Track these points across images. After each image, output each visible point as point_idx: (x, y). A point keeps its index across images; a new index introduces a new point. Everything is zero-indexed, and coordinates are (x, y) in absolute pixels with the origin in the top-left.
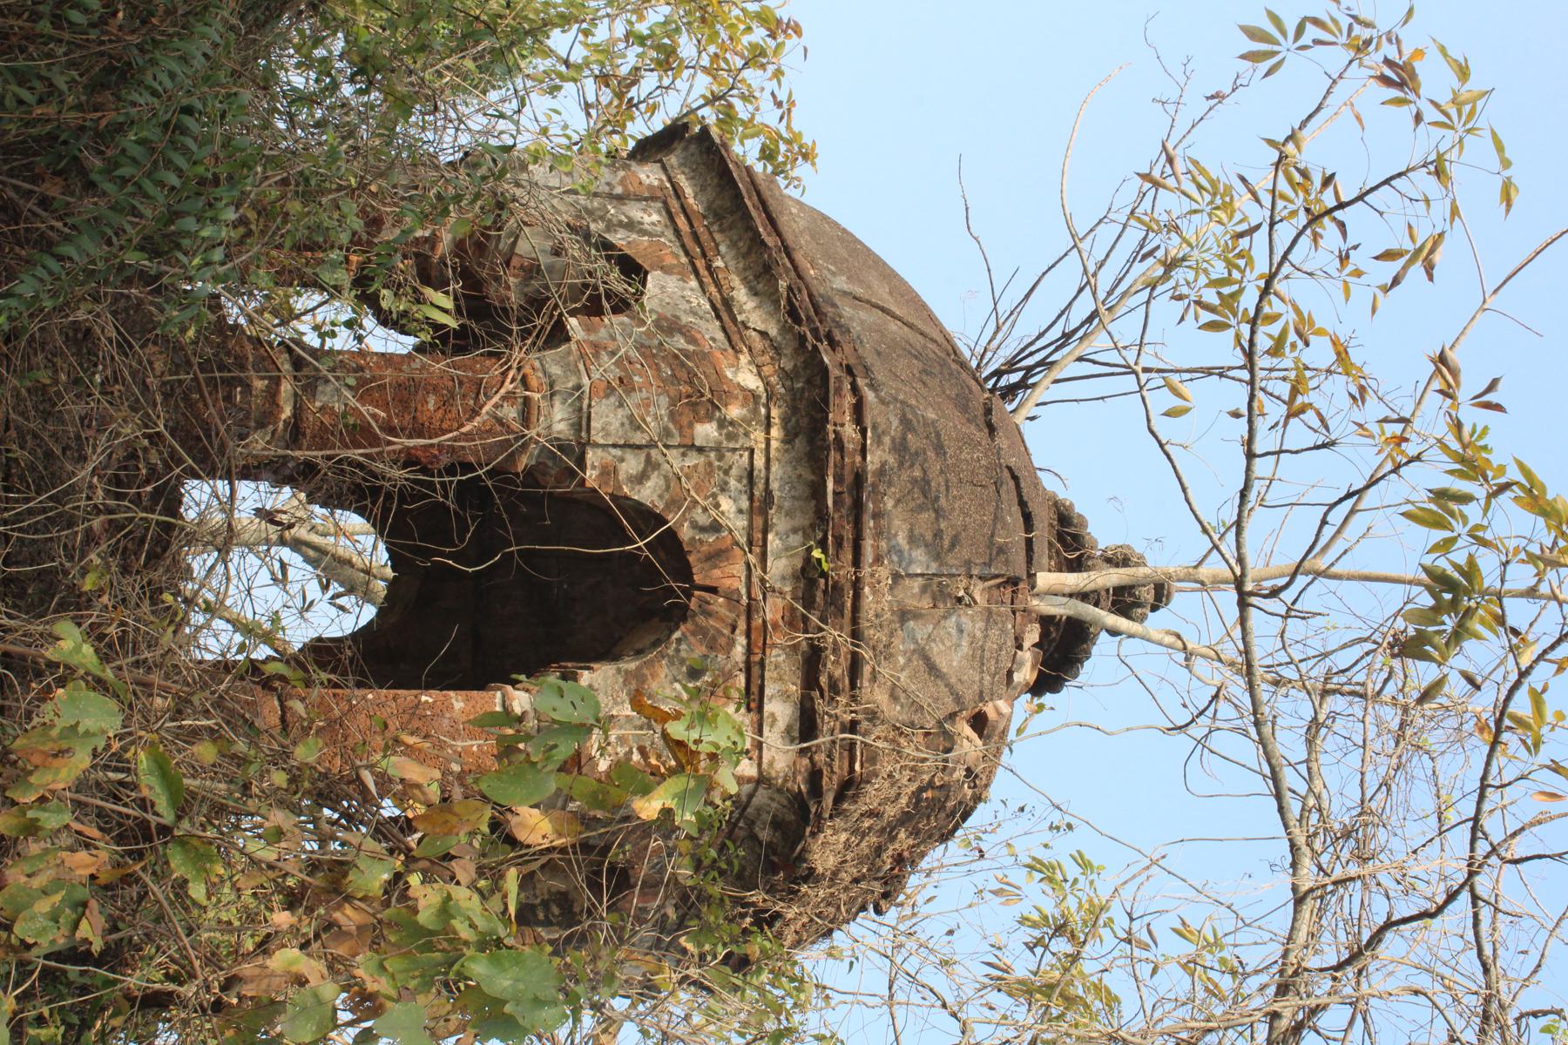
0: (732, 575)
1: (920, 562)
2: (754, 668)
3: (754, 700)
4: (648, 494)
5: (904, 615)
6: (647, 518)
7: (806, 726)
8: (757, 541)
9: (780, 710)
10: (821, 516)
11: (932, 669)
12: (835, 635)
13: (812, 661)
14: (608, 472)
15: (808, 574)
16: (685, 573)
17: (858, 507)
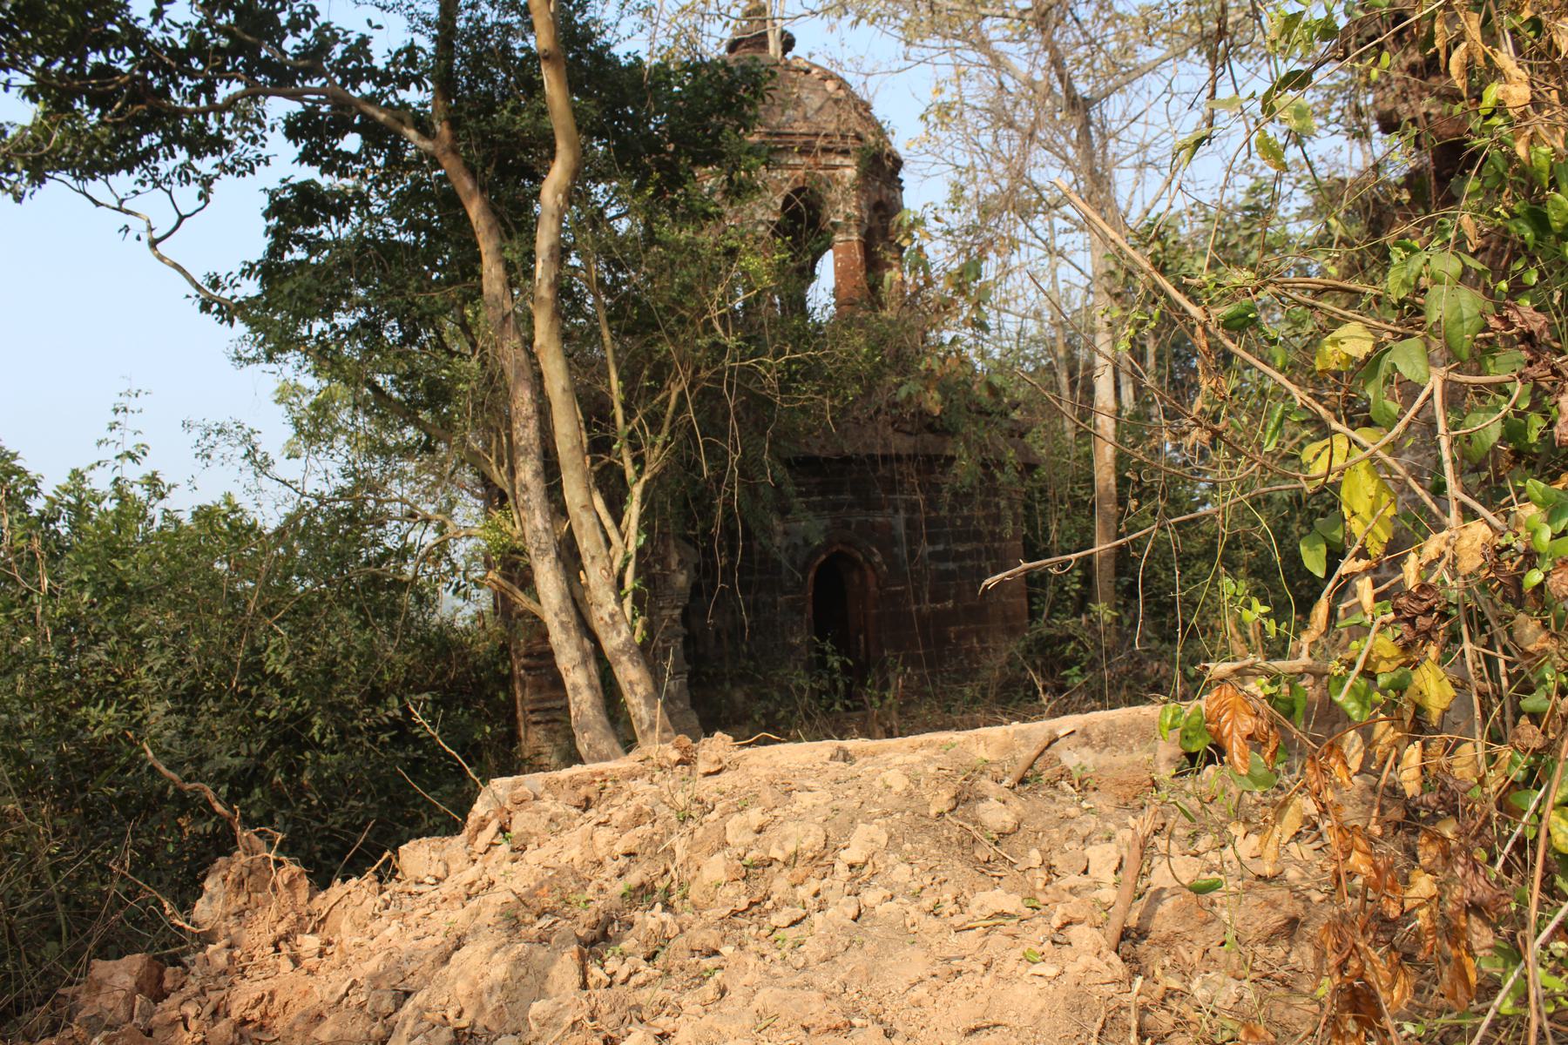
0: (801, 173)
1: (790, 112)
2: (827, 167)
3: (836, 167)
4: (780, 202)
5: (806, 118)
6: (788, 201)
7: (845, 153)
8: (795, 167)
9: (838, 160)
10: (785, 149)
11: (821, 108)
12: (820, 142)
13: (826, 150)
14: (775, 214)
15: (802, 152)
16: (803, 189)
17: (778, 135)
